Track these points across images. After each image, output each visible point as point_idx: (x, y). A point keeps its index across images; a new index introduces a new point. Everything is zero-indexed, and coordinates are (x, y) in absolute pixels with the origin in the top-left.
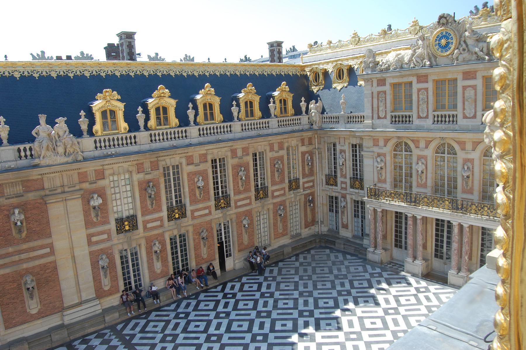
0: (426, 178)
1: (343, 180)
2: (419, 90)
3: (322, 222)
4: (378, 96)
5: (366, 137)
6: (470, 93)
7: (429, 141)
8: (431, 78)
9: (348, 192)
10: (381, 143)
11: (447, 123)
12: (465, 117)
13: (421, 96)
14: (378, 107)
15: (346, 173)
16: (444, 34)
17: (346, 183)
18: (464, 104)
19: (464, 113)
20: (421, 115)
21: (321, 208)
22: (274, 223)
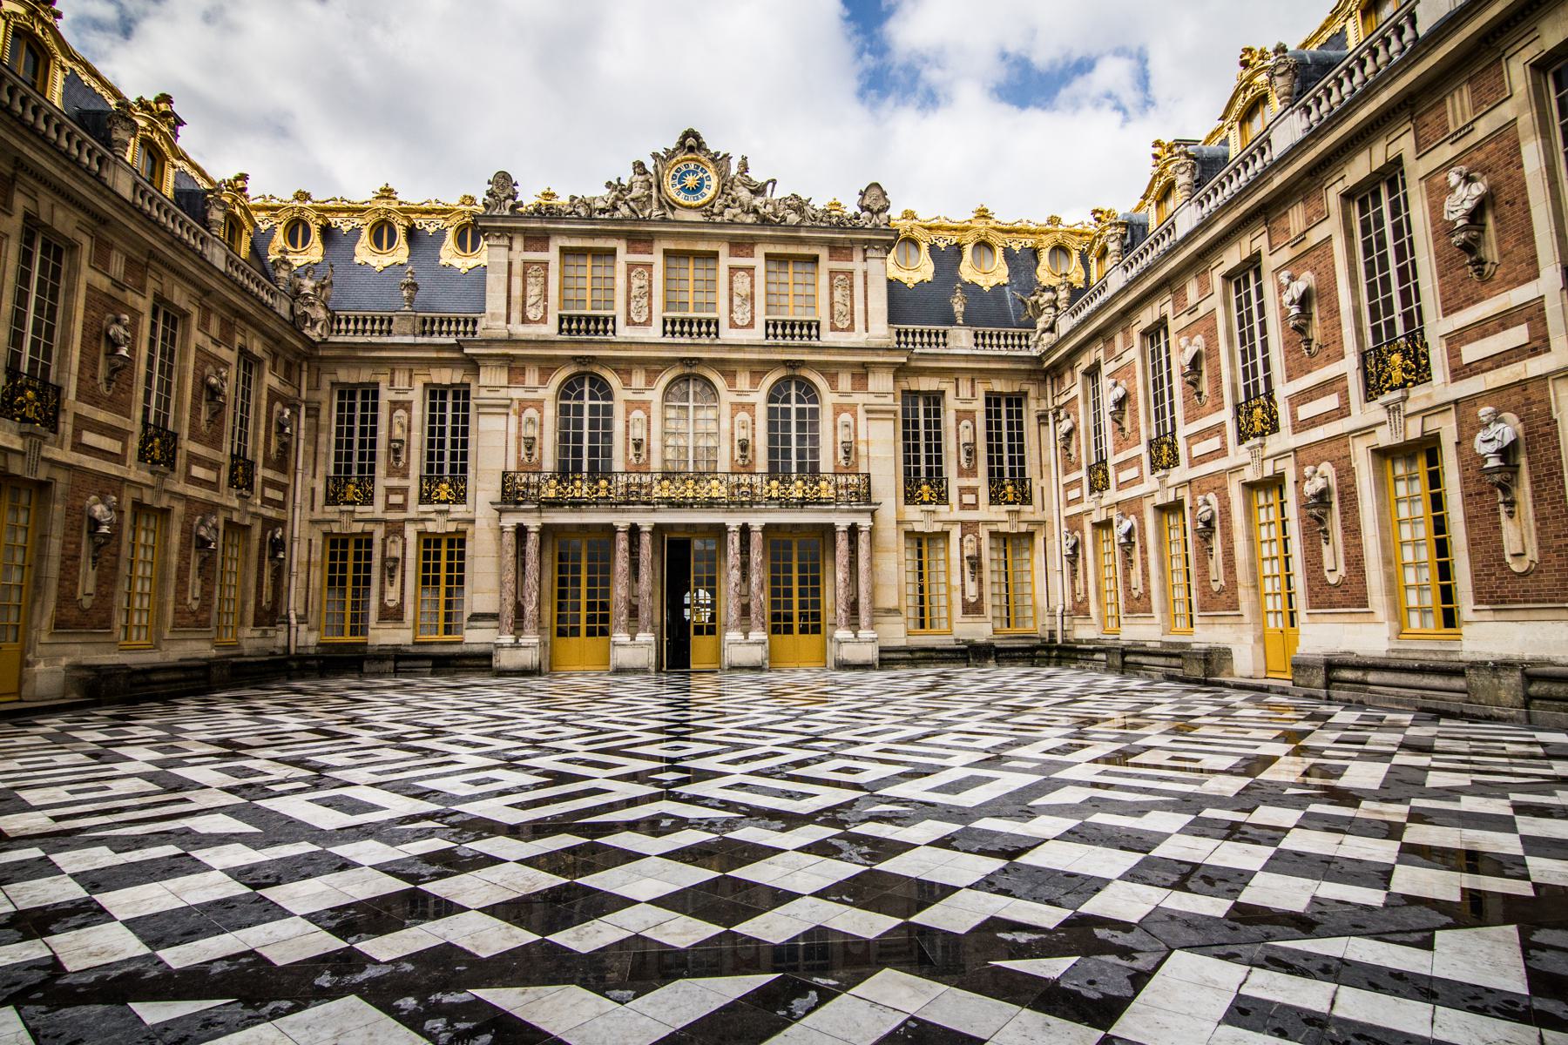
1: (395, 482)
3: (302, 619)
4: (525, 273)
8: (660, 246)
9: (412, 514)
10: (532, 378)
12: (733, 325)
13: (636, 283)
14: (524, 297)
15: (407, 463)
17: (404, 491)
18: (731, 300)
19: (731, 319)
20: (636, 319)
21: (303, 576)
22: (179, 568)
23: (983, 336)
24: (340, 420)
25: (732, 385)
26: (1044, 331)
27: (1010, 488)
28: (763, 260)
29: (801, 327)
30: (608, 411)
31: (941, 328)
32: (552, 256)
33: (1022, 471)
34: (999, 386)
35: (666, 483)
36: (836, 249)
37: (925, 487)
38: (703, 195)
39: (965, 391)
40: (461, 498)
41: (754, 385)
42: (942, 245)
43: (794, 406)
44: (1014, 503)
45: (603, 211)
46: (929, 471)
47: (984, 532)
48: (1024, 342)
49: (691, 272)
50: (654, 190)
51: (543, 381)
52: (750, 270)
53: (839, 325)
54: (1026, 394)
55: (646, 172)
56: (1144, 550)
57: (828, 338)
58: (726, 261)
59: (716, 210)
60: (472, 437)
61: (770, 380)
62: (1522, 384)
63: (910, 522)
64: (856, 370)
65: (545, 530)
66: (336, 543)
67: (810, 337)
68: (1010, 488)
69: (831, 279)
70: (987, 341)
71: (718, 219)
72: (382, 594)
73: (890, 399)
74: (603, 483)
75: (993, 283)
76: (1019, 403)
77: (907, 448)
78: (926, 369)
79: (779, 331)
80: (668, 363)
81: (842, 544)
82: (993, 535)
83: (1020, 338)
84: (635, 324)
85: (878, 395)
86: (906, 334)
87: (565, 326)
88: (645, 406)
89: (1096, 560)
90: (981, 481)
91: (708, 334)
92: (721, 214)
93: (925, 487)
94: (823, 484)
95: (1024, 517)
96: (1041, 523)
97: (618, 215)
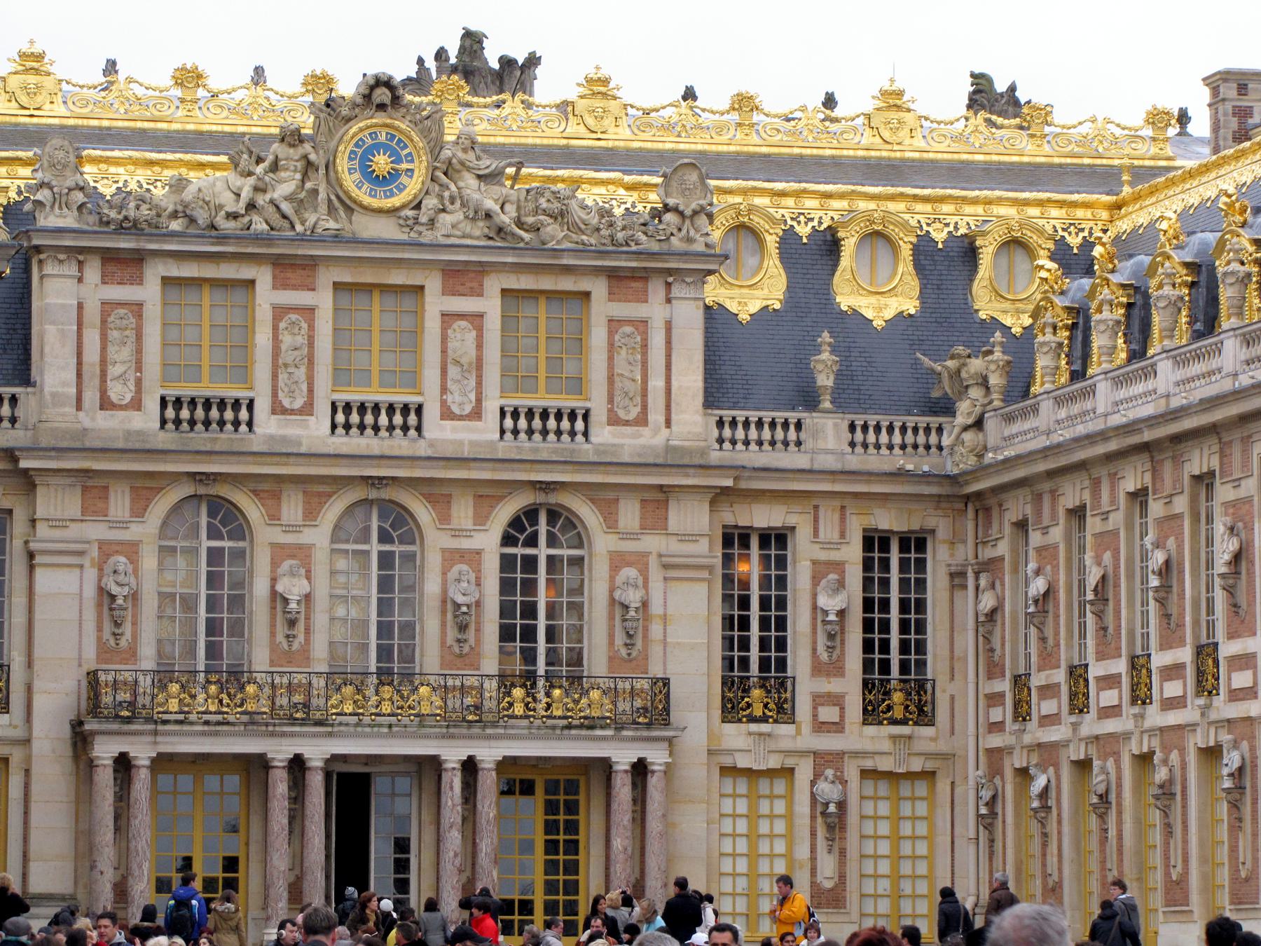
0: (308, 631)
2: (280, 312)
4: (104, 322)
5: (53, 480)
6: (463, 340)
7: (319, 494)
8: (327, 277)
10: (119, 503)
11: (383, 433)
12: (447, 414)
13: (287, 340)
14: (103, 362)
16: (382, 138)
18: (444, 372)
19: (444, 403)
20: (286, 403)
23: (865, 428)
25: (444, 518)
26: (966, 428)
27: (897, 697)
28: (497, 301)
29: (559, 416)
30: (239, 555)
31: (793, 416)
32: (149, 291)
33: (921, 665)
34: (886, 520)
35: (348, 690)
37: (757, 693)
38: (401, 188)
39: (828, 530)
41: (481, 519)
42: (804, 230)
43: (542, 552)
44: (904, 722)
45: (234, 216)
46: (764, 664)
47: (852, 773)
48: (933, 439)
49: (377, 314)
51: (139, 511)
52: (476, 319)
53: (622, 414)
54: (933, 532)
55: (301, 140)
56: (1059, 822)
58: (436, 302)
59: (423, 219)
60: (17, 601)
62: (1249, 719)
63: (730, 752)
64: (647, 496)
65: (162, 762)
67: (573, 433)
68: (897, 697)
69: (611, 334)
70: (871, 437)
71: (427, 237)
73: (702, 546)
74: (251, 689)
75: (889, 314)
76: (921, 545)
77: (728, 621)
78: (763, 492)
79: (522, 423)
81: (623, 790)
82: (865, 774)
83: (927, 430)
84: (285, 411)
85: (684, 537)
86: (734, 423)
87: (170, 413)
88: (302, 554)
89: (1017, 826)
90: (850, 684)
91: (405, 428)
92: (432, 222)
93: (757, 693)
94: (595, 694)
95: (919, 746)
97: (260, 226)
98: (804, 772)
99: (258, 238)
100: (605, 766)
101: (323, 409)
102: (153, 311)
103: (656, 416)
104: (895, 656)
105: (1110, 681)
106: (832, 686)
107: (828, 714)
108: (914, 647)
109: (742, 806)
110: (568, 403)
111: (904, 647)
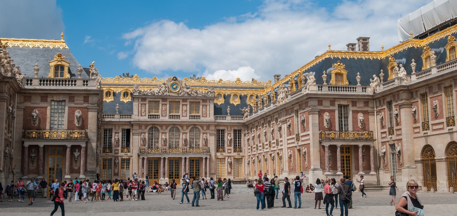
6: (185, 108)
10: (143, 127)
12: (183, 116)
13: (164, 108)
24: (104, 136)
25: (183, 129)
32: (147, 102)
34: (236, 128)
36: (204, 101)
39: (229, 129)
40: (129, 152)
41: (187, 129)
50: (167, 89)
57: (202, 119)
58: (181, 103)
61: (190, 128)
66: (104, 160)
71: (180, 95)
72: (114, 170)
76: (240, 131)
77: (217, 141)
80: (170, 125)
81: (204, 161)
90: (232, 148)
96: (244, 156)
97: (160, 94)
98: (227, 158)
99: (160, 96)
100: (202, 158)
101: (168, 116)
102: (147, 105)
103: (208, 116)
104: (237, 144)
105: (260, 146)
106: (230, 148)
107: (229, 151)
108: (240, 143)
109: (219, 162)
110: (197, 114)
111: (239, 143)
